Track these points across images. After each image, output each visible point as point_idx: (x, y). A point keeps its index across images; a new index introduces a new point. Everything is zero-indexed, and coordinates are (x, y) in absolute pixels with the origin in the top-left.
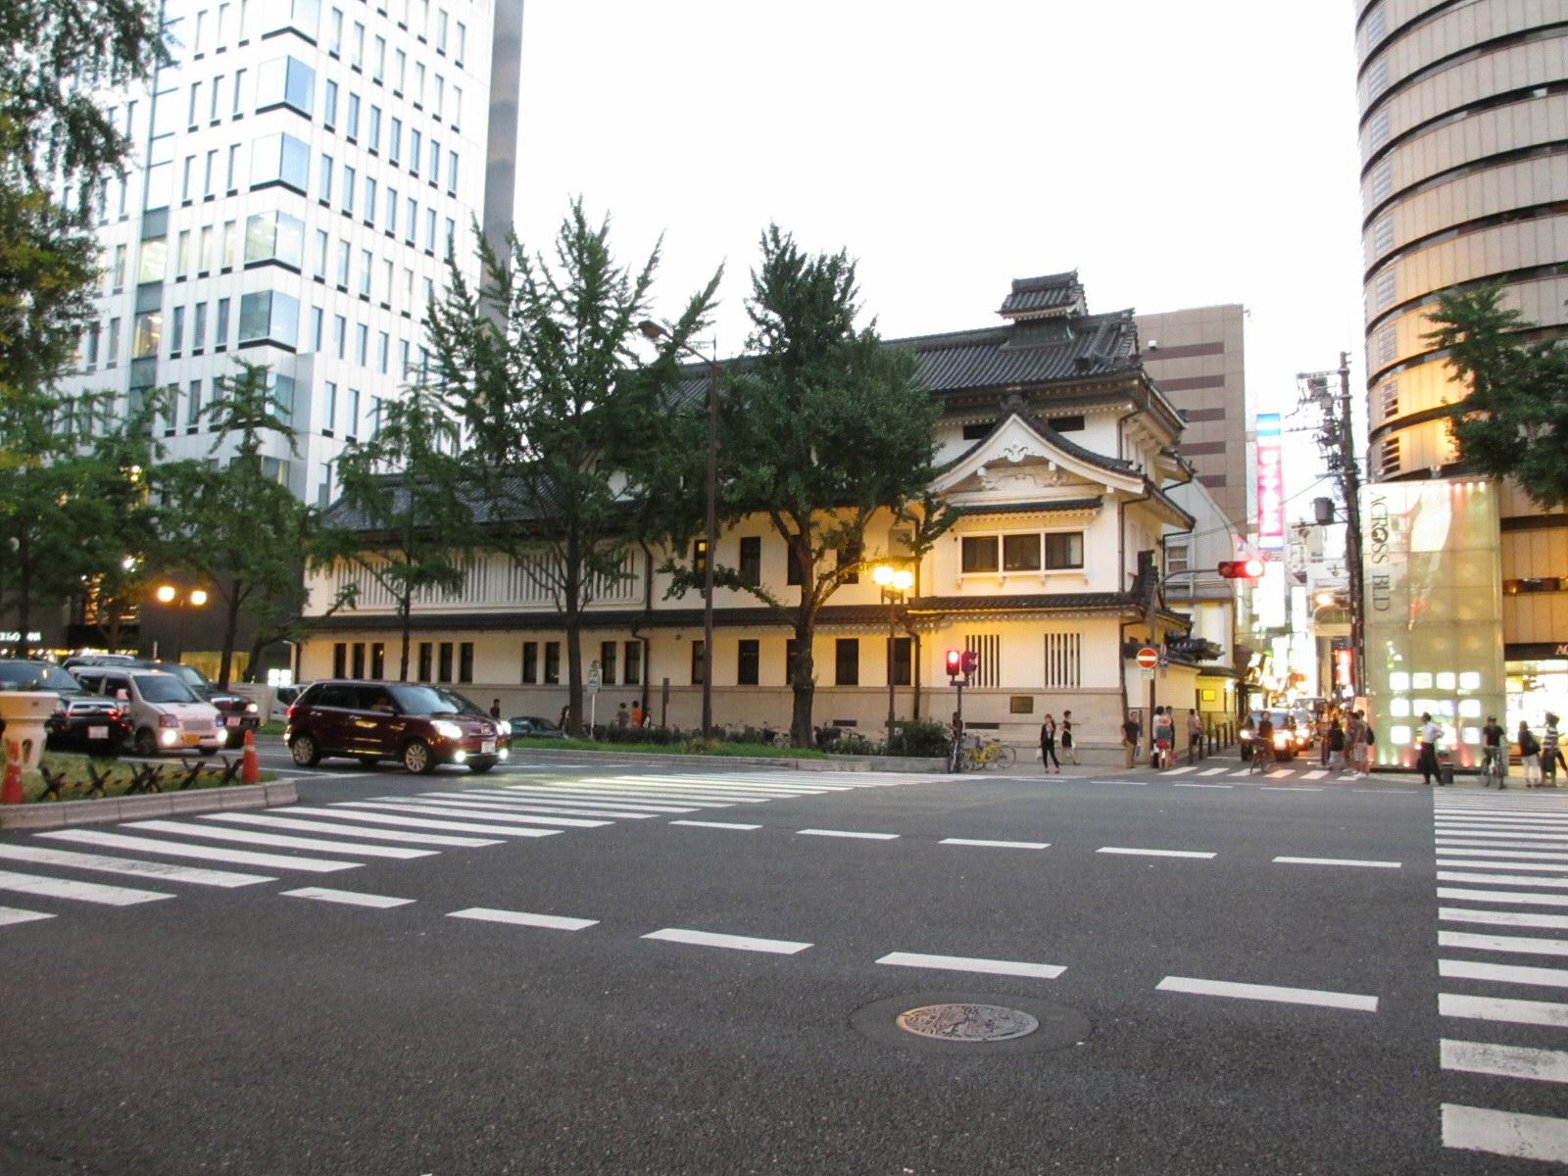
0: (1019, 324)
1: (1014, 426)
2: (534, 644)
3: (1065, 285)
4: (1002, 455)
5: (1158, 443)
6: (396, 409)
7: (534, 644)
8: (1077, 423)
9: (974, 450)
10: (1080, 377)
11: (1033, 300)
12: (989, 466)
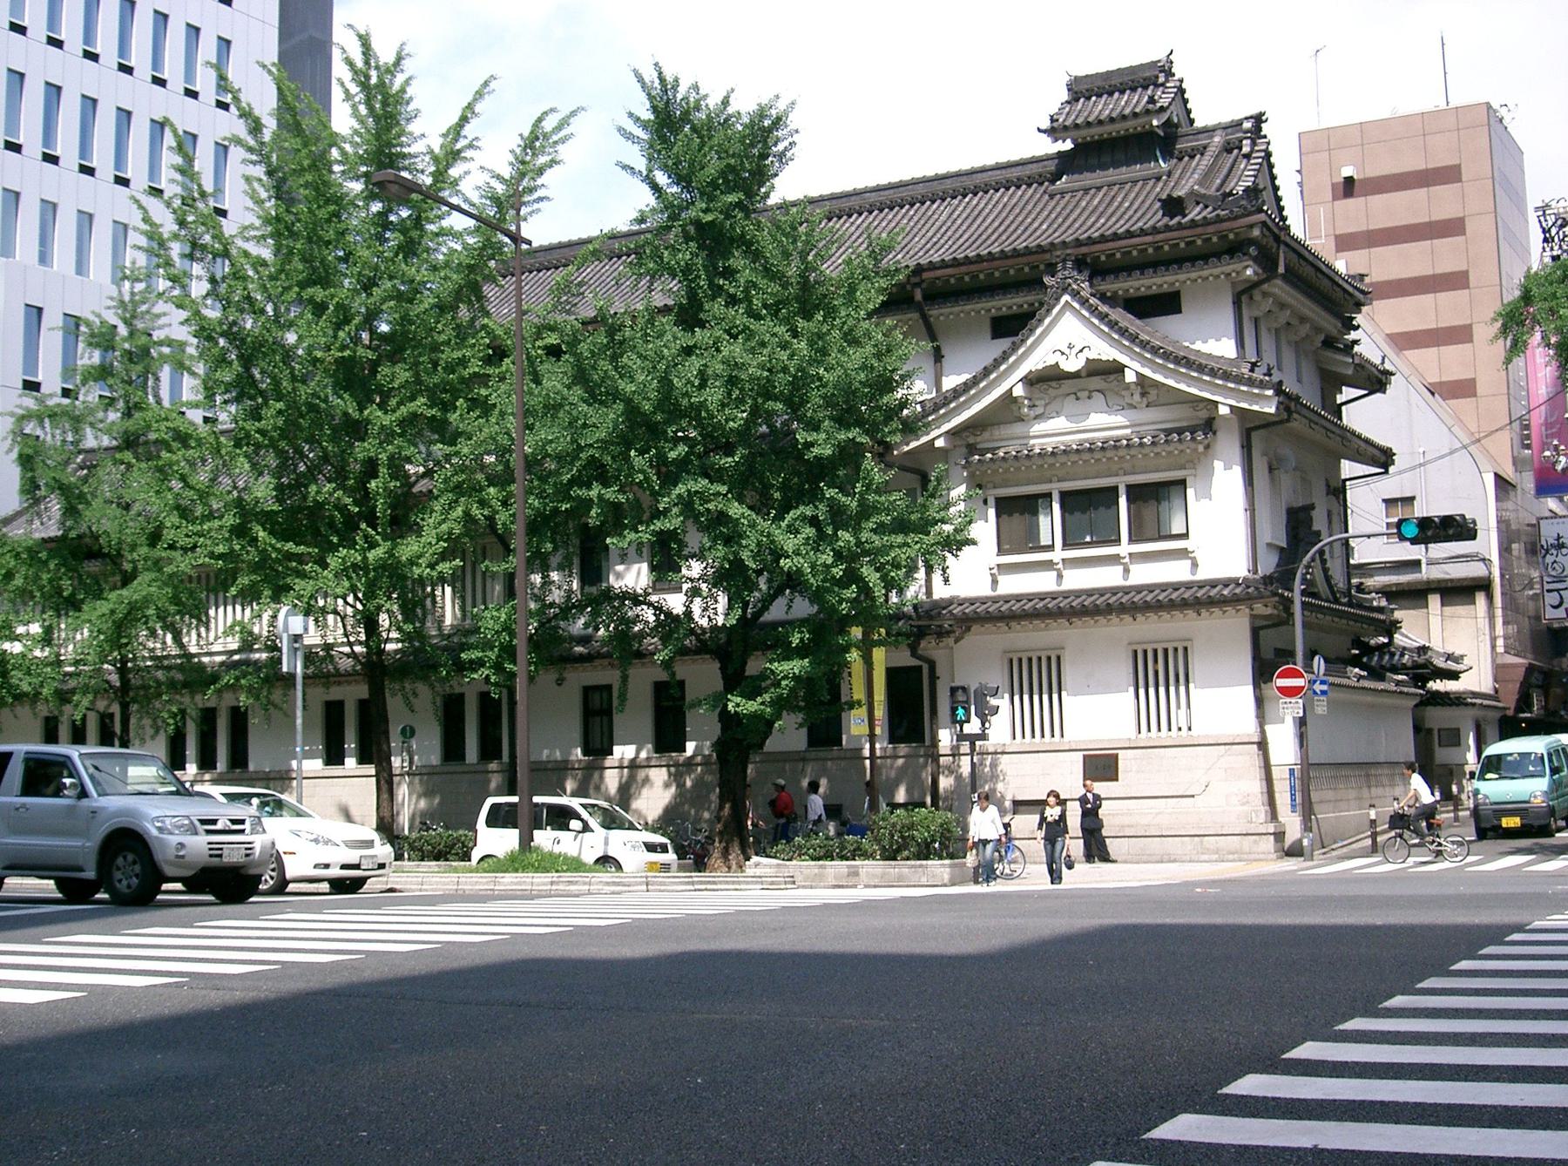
0: (1080, 148)
1: (1068, 315)
2: (341, 704)
3: (1153, 76)
4: (1051, 362)
5: (1318, 330)
6: (104, 339)
7: (341, 704)
8: (1168, 304)
9: (1005, 357)
10: (1168, 228)
11: (1102, 108)
12: (1031, 381)
